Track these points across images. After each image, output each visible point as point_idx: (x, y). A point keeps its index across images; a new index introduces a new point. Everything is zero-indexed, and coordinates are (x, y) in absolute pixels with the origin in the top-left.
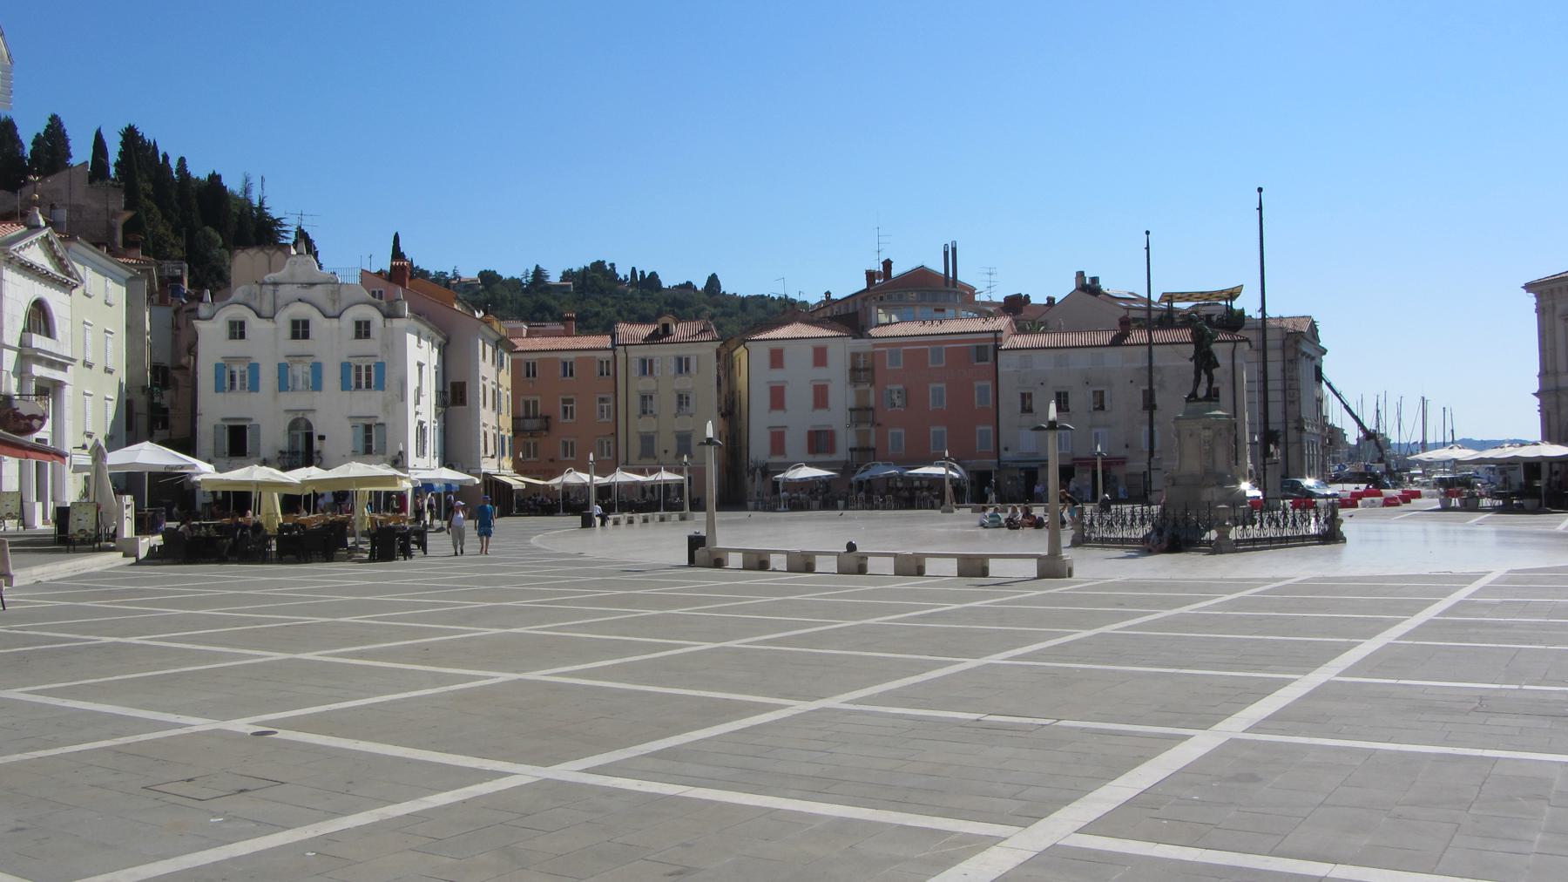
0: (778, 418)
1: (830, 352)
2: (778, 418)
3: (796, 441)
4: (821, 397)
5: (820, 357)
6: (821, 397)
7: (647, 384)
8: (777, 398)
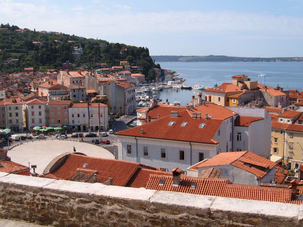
0: (33, 117)
1: (41, 106)
2: (33, 117)
3: (37, 121)
4: (40, 114)
5: (40, 107)
6: (40, 114)
7: (10, 111)
8: (33, 114)
